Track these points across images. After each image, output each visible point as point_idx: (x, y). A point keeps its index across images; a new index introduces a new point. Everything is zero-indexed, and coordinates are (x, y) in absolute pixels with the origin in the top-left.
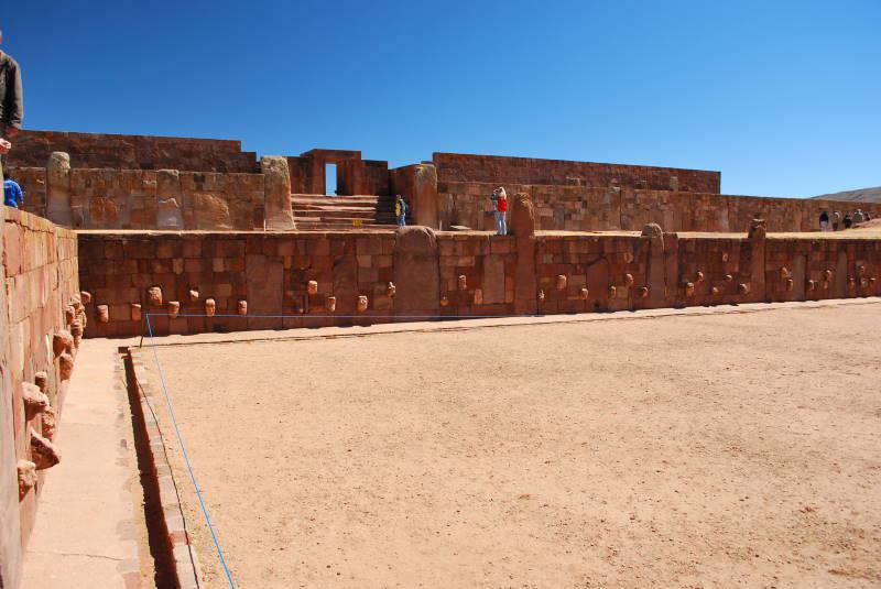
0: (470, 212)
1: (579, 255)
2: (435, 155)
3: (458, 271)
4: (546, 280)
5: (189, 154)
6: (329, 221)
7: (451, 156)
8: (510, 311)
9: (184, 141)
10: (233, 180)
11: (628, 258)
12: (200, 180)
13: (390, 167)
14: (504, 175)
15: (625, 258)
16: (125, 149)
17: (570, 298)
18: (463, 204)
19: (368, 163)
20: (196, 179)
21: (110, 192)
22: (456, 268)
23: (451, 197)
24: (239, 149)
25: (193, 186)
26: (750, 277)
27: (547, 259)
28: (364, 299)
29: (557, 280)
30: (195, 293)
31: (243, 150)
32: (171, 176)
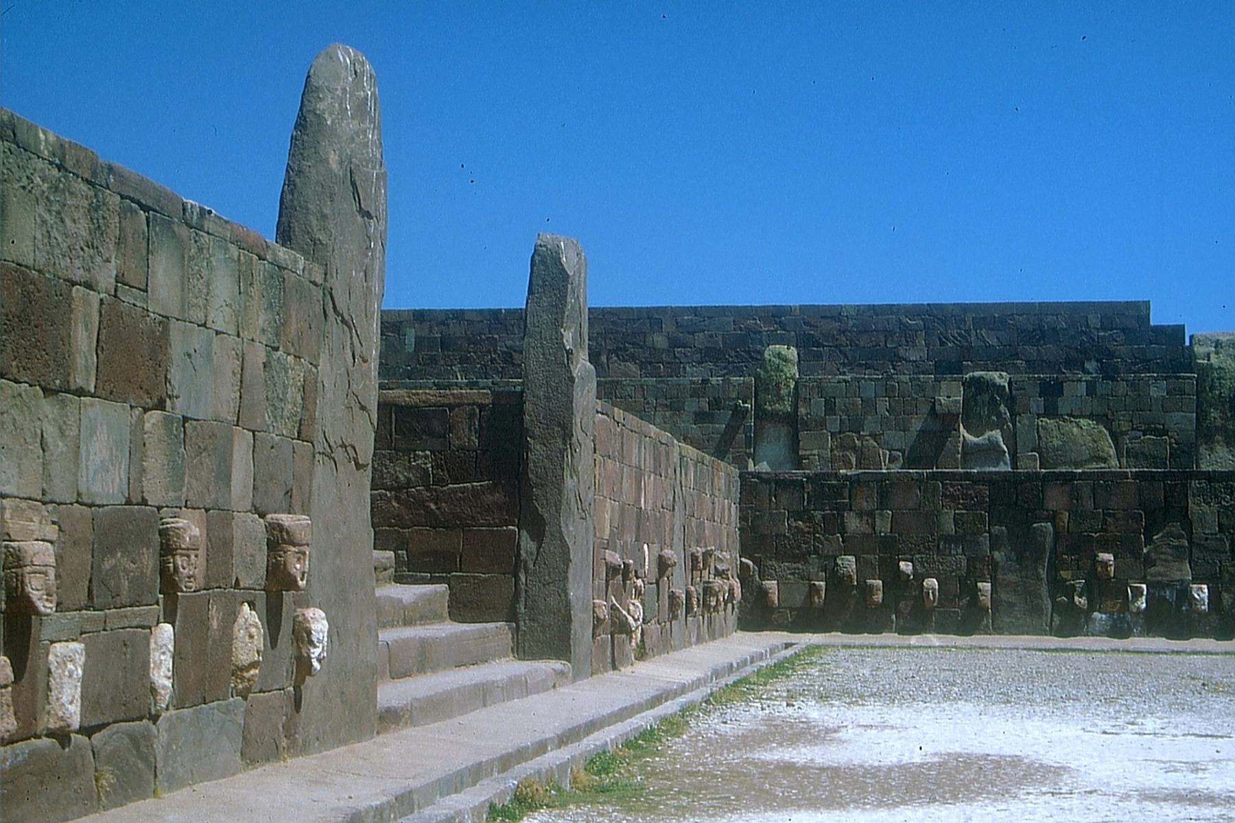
12: (1052, 391)
16: (908, 335)
21: (870, 425)
25: (1037, 403)
28: (1202, 593)
30: (906, 566)
31: (1152, 324)
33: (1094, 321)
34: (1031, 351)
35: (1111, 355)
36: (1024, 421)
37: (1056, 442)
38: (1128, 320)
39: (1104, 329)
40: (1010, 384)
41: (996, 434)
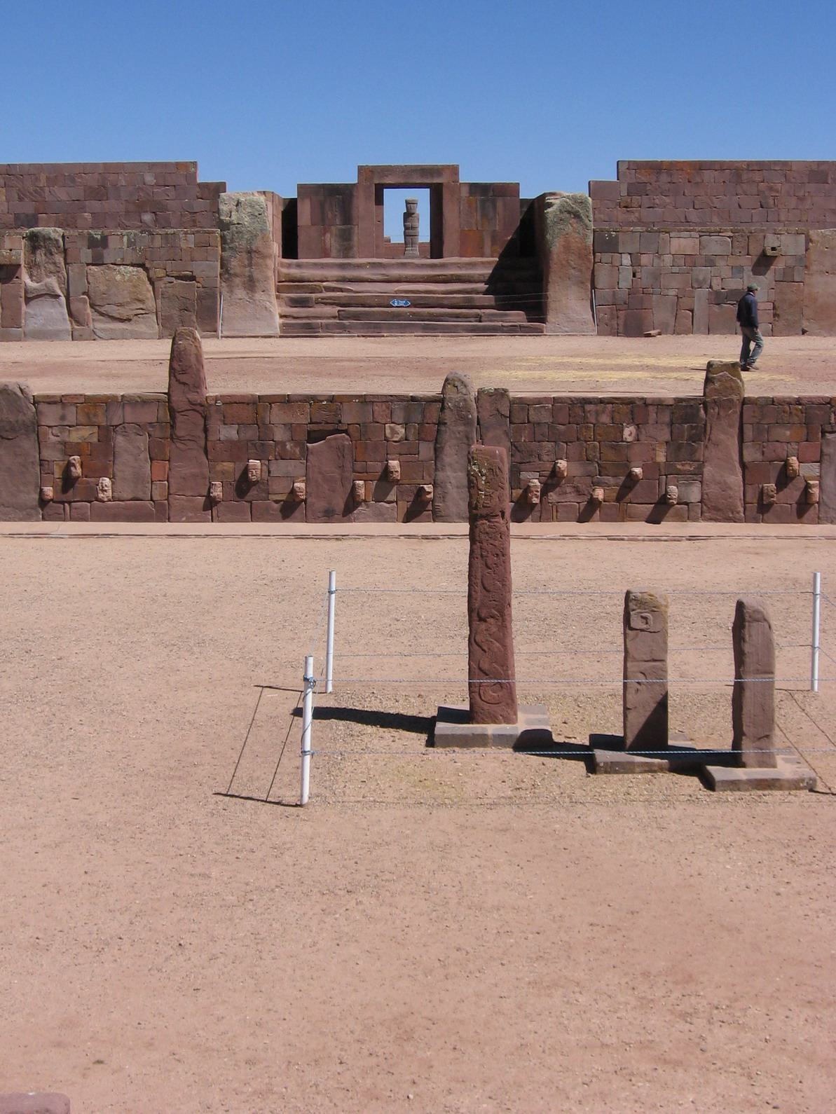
0: (672, 292)
1: (289, 427)
2: (628, 168)
3: (68, 448)
4: (228, 466)
5: (99, 193)
6: (356, 316)
7: (656, 168)
8: (162, 513)
9: (85, 169)
10: (158, 242)
11: (394, 432)
12: (98, 245)
13: (524, 195)
14: (793, 202)
15: (388, 431)
17: (270, 497)
18: (656, 276)
19: (476, 188)
20: (92, 243)
22: (65, 443)
23: (626, 260)
24: (194, 175)
25: (86, 254)
26: (698, 473)
27: (229, 433)
29: (246, 470)
32: (47, 239)
33: (150, 179)
34: (95, 205)
35: (164, 209)
36: (74, 269)
37: (103, 288)
38: (178, 175)
39: (158, 185)
40: (63, 237)
41: (53, 282)
